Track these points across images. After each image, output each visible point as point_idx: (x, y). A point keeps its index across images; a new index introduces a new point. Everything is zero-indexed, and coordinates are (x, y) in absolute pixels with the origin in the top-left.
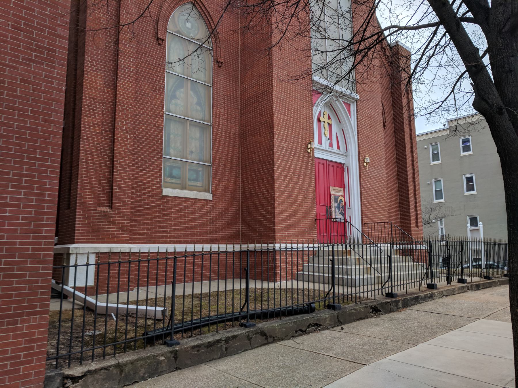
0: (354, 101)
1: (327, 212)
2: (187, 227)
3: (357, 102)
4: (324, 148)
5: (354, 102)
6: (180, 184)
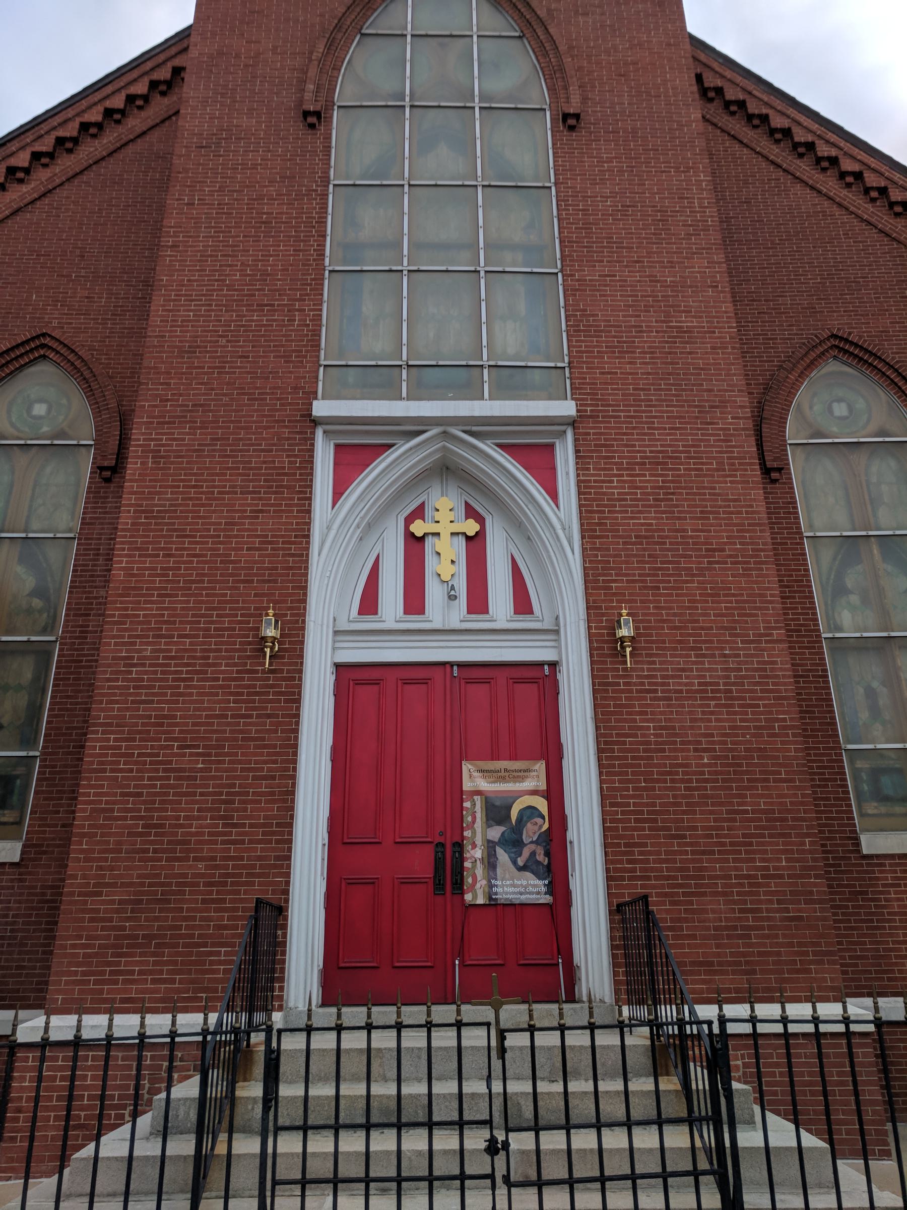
0: (563, 428)
1: (439, 864)
4: (437, 624)
5: (565, 432)
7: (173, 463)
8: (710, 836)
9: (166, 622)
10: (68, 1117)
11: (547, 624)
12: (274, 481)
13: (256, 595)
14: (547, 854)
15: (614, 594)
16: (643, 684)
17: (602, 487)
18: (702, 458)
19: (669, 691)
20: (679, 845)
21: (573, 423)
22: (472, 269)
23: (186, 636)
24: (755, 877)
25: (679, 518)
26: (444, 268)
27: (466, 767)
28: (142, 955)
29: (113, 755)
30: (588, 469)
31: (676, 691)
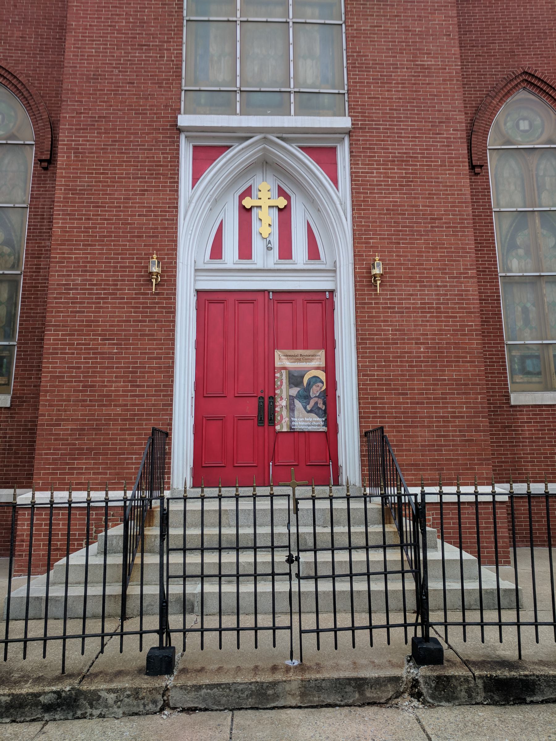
1: (261, 409)
4: (260, 266)
7: (88, 157)
8: (423, 394)
9: (88, 262)
10: (50, 545)
11: (328, 267)
12: (154, 170)
13: (145, 245)
14: (324, 403)
15: (372, 247)
16: (386, 303)
17: (366, 177)
18: (431, 158)
19: (402, 308)
20: (403, 399)
21: (349, 133)
22: (284, 20)
23: (102, 271)
24: (447, 417)
25: (415, 198)
26: (264, 19)
27: (277, 353)
28: (86, 459)
29: (62, 344)
30: (358, 164)
31: (407, 308)
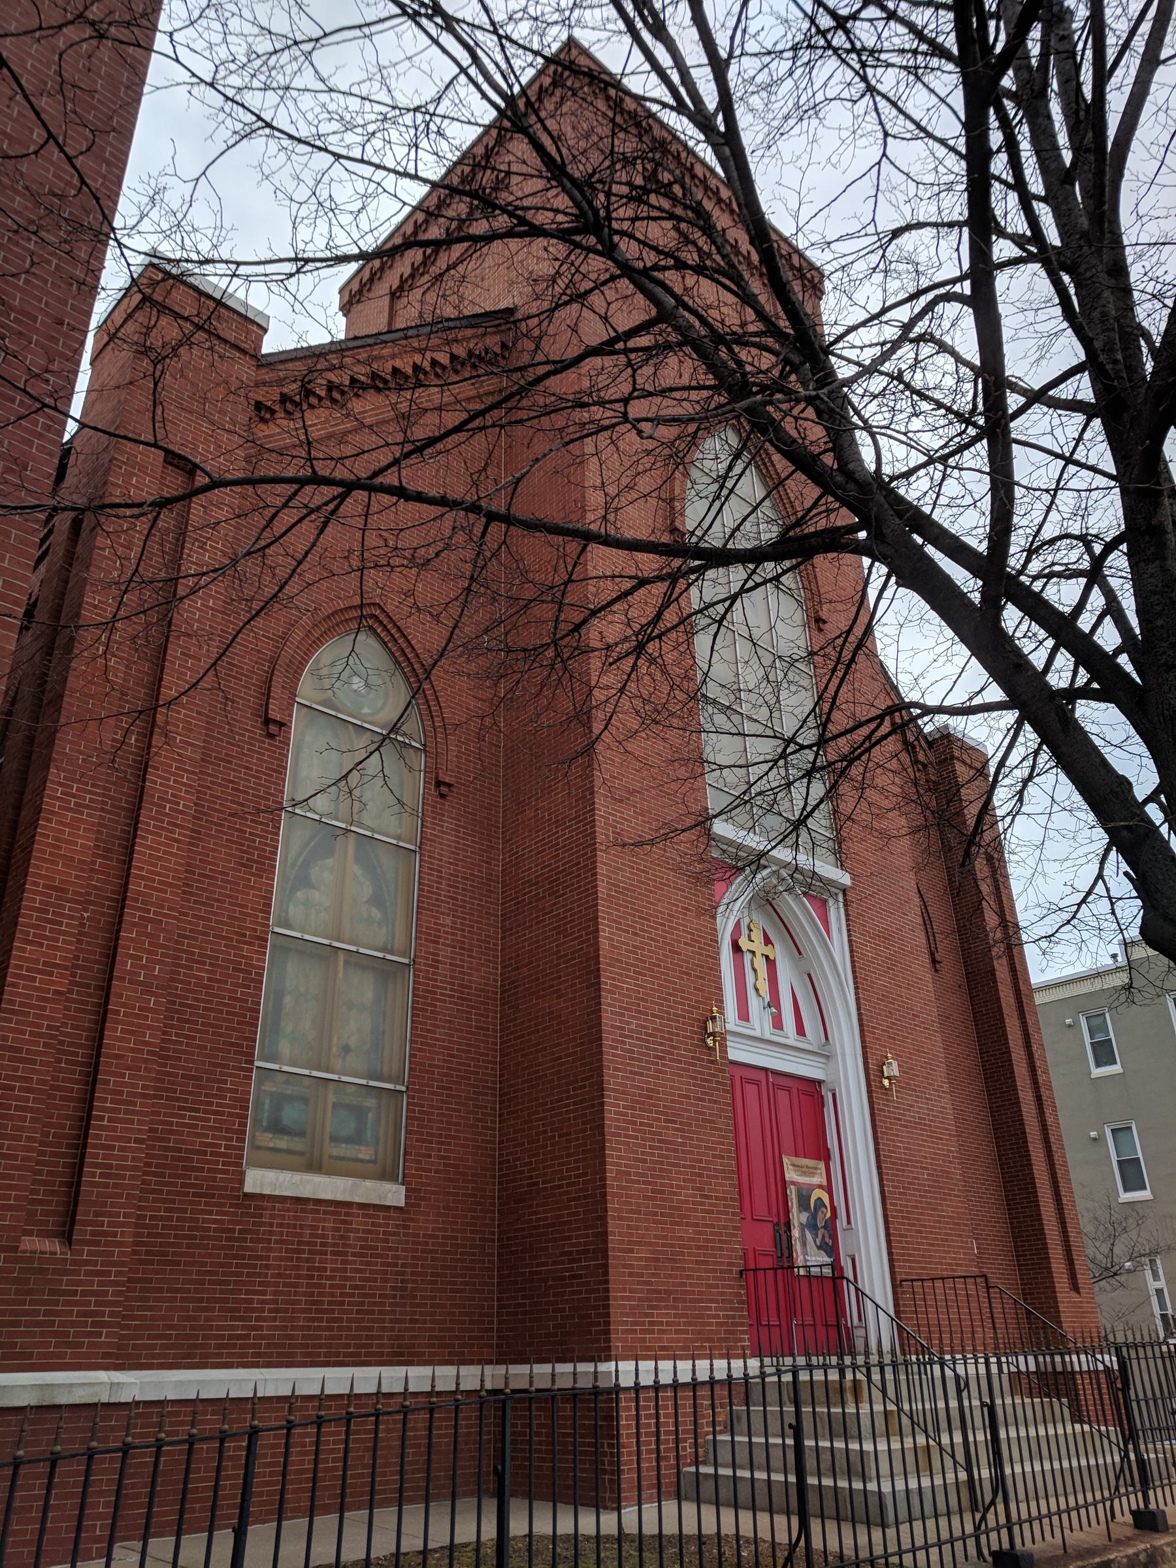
1: (777, 1241)
2: (314, 1303)
3: (845, 895)
4: (757, 1034)
6: (302, 1154)
